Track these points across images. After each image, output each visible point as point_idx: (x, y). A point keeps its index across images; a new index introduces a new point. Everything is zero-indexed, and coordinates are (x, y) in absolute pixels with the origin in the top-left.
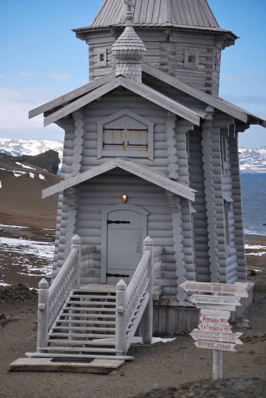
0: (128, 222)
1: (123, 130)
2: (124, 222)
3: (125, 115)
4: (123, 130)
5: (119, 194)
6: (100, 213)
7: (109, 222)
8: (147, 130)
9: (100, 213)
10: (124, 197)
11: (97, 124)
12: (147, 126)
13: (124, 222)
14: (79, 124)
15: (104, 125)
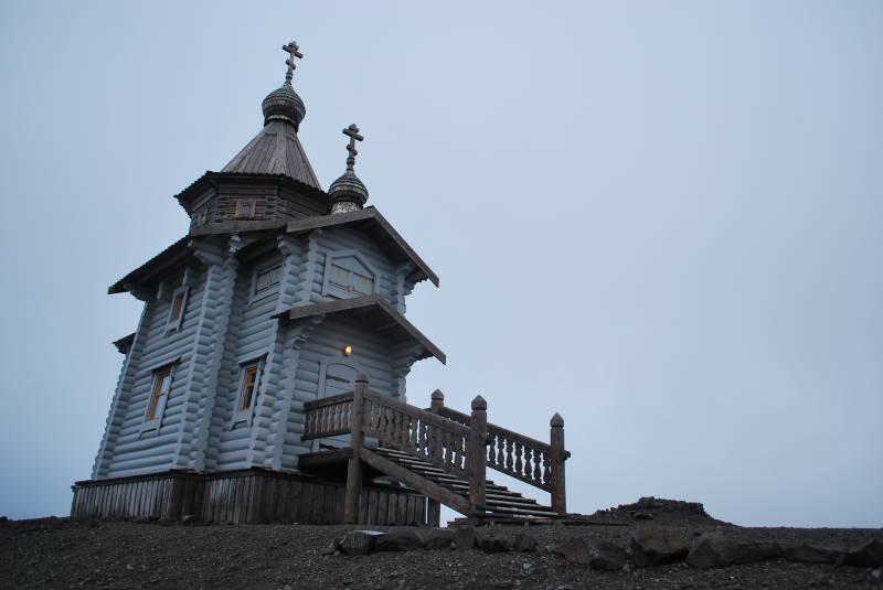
0: (348, 382)
1: (349, 271)
2: (344, 381)
3: (355, 257)
4: (349, 271)
5: (340, 345)
6: (319, 363)
7: (328, 377)
8: (373, 280)
9: (319, 363)
10: (349, 350)
11: (325, 255)
12: (373, 275)
13: (344, 381)
14: (313, 245)
15: (334, 258)
